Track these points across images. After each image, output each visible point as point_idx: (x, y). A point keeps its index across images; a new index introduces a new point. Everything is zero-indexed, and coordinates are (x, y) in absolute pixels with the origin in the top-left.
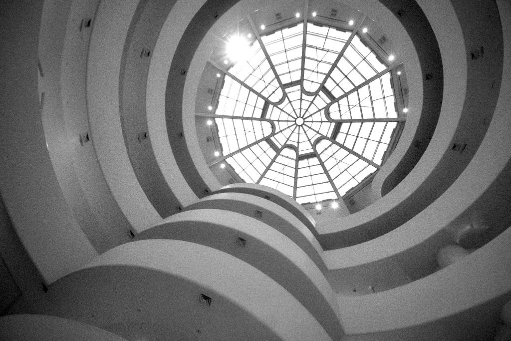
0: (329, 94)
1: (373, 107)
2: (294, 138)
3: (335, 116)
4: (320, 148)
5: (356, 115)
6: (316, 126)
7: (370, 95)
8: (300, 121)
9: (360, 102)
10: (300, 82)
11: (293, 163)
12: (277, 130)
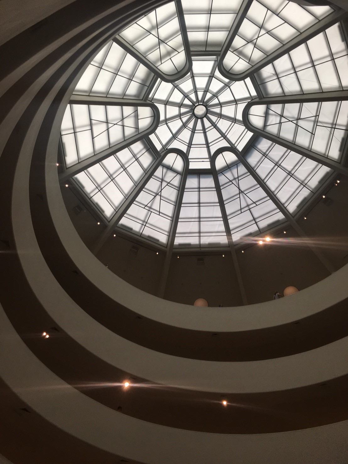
0: (150, 147)
1: (91, 120)
2: (216, 86)
3: (145, 112)
4: (180, 58)
5: (114, 112)
6: (177, 97)
7: (93, 138)
8: (200, 110)
9: (108, 129)
10: (187, 173)
11: (238, 42)
12: (241, 107)
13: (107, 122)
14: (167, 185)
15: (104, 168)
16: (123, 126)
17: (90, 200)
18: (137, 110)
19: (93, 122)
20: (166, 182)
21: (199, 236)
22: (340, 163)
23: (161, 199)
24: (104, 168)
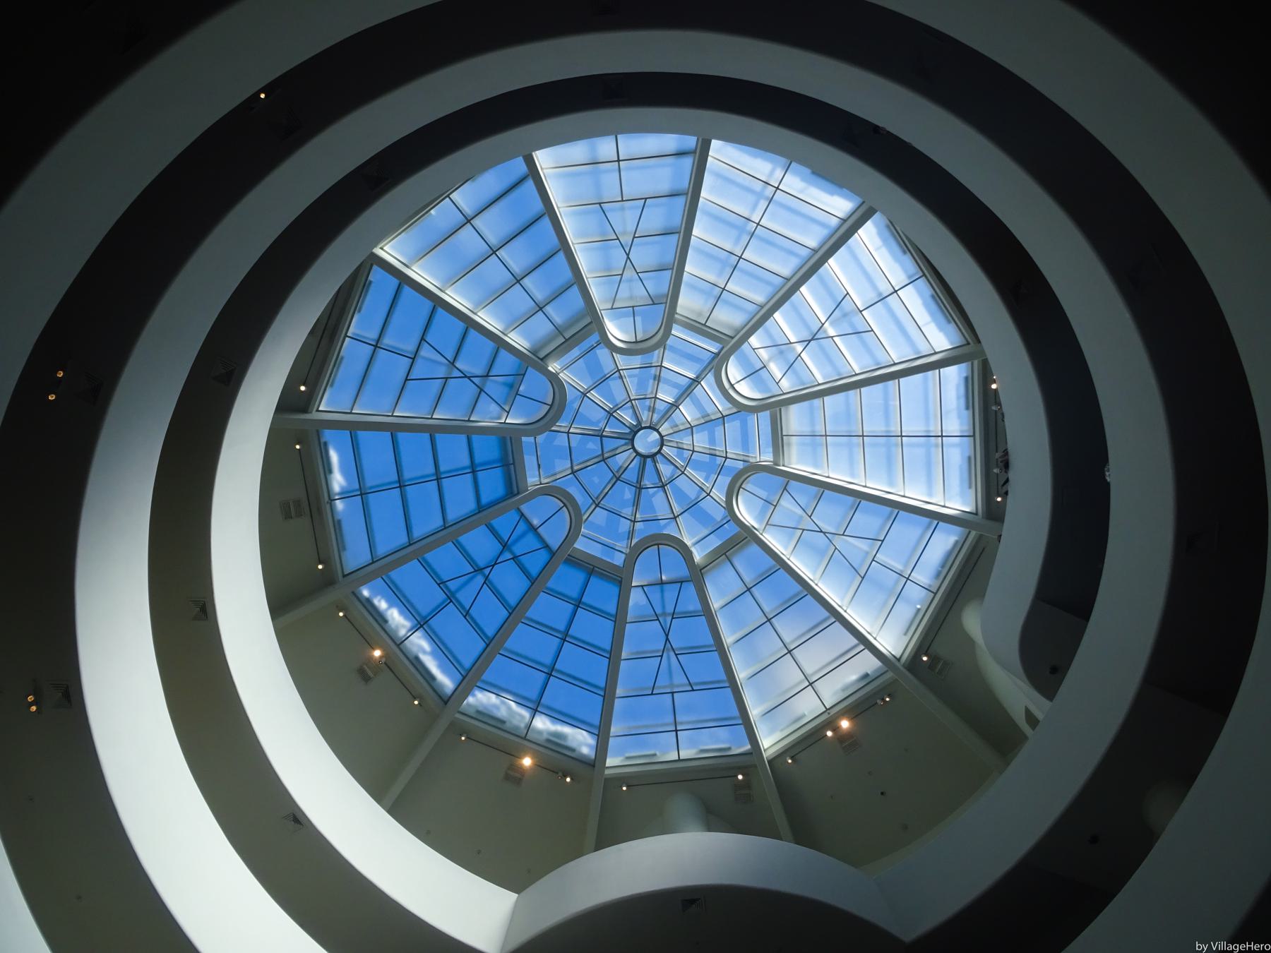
1: (441, 584)
7: (467, 614)
13: (478, 570)
14: (673, 618)
15: (518, 658)
16: (515, 558)
17: (529, 740)
18: (522, 515)
19: (452, 585)
20: (669, 614)
21: (548, 674)
22: (968, 344)
23: (676, 655)
24: (518, 658)
